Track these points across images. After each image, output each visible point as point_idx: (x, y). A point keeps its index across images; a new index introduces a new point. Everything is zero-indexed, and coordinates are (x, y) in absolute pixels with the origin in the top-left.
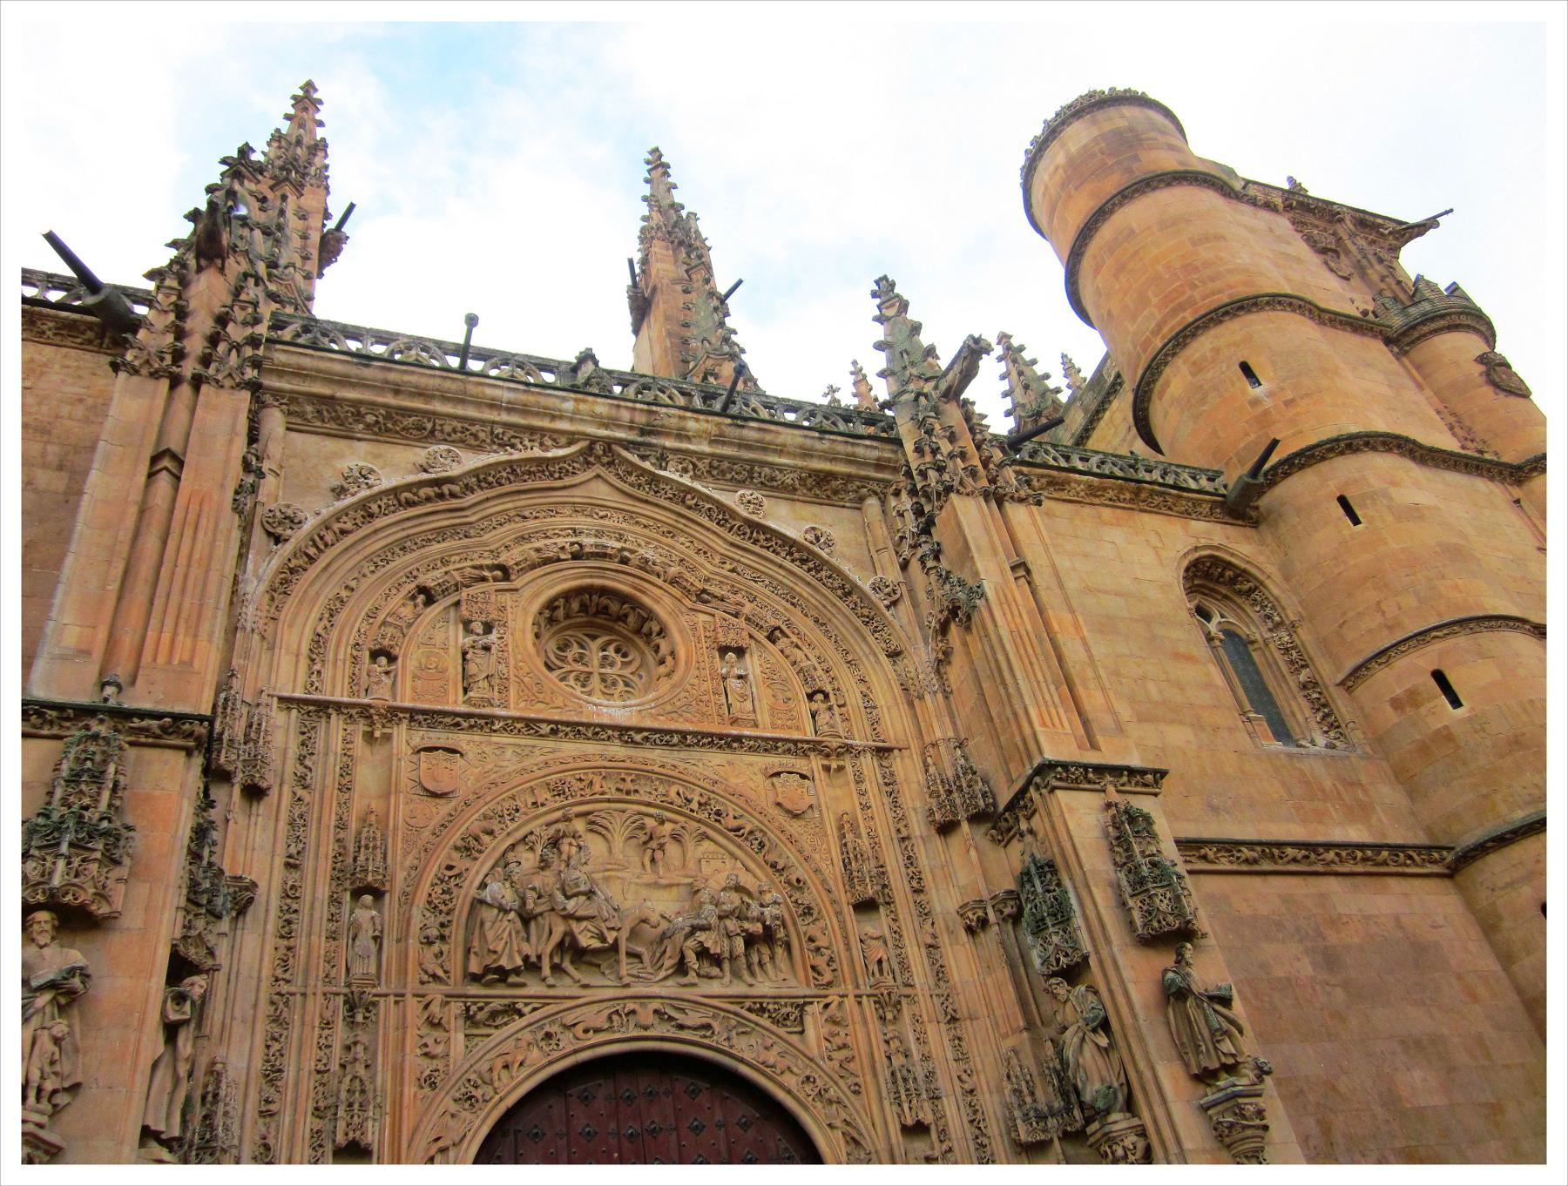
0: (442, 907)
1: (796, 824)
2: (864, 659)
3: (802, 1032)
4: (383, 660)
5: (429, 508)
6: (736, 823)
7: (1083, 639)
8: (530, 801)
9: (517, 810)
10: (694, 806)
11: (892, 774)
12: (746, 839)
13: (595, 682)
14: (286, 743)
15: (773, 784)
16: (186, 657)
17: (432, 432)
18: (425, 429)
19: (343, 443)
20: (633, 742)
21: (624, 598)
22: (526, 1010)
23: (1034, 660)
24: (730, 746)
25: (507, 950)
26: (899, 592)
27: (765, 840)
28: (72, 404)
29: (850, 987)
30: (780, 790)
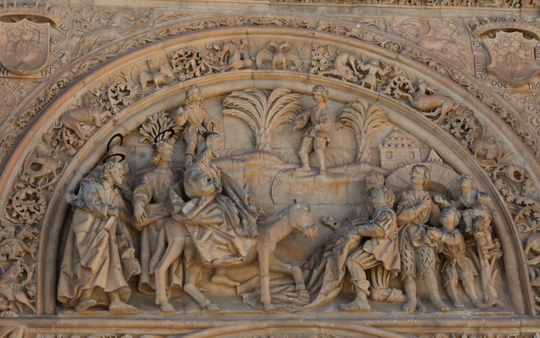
0: (25, 215)
8: (145, 78)
9: (127, 92)
10: (371, 80)
12: (445, 122)
15: (484, 46)
27: (471, 123)
30: (493, 54)
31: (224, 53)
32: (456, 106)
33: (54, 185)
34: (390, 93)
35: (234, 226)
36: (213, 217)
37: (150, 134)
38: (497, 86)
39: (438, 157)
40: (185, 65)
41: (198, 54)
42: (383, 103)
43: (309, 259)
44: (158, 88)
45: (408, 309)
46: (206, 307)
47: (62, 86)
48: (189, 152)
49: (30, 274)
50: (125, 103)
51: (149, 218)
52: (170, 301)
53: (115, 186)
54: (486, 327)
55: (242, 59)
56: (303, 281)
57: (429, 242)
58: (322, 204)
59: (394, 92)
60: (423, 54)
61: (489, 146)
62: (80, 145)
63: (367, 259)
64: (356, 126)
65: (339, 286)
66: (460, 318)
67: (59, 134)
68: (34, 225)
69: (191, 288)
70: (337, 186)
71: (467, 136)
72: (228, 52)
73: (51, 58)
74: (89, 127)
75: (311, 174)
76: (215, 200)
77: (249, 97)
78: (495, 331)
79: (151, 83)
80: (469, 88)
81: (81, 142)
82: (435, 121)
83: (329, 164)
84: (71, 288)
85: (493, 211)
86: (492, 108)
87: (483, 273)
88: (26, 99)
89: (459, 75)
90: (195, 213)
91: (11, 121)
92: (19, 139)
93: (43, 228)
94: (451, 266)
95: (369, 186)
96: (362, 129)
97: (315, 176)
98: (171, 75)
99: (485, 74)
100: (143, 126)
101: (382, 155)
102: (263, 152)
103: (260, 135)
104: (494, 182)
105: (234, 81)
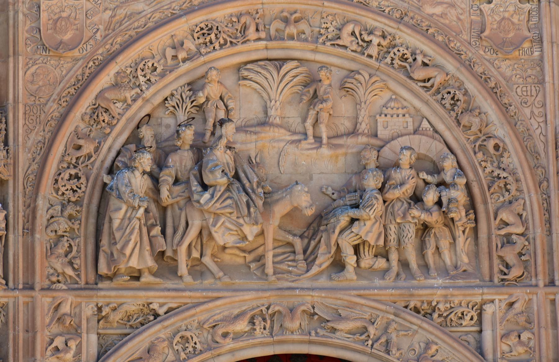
0: (69, 194)
1: (506, 67)
3: (481, 331)
8: (170, 53)
10: (373, 50)
22: (161, 311)
27: (459, 95)
29: (541, 284)
30: (489, 20)
31: (241, 25)
32: (449, 76)
33: (93, 164)
34: (389, 62)
35: (243, 216)
36: (226, 207)
37: (174, 107)
38: (489, 53)
39: (429, 126)
40: (205, 39)
41: (217, 27)
42: (383, 73)
43: (309, 226)
44: (181, 64)
45: (388, 278)
46: (220, 278)
47: (97, 64)
48: (208, 128)
49: (75, 249)
50: (153, 80)
51: (173, 198)
52: (190, 273)
53: (144, 173)
54: (453, 295)
55: (257, 30)
56: (302, 252)
57: (410, 219)
58: (323, 173)
59: (394, 62)
60: (424, 20)
61: (474, 119)
62: (113, 124)
63: (355, 238)
64: (357, 96)
65: (332, 257)
66: (432, 287)
67: (96, 114)
68: (76, 203)
69: (207, 260)
70: (337, 157)
71: (456, 108)
72: (245, 23)
73: (87, 34)
74: (121, 104)
75: (314, 146)
76: (228, 189)
77: (262, 71)
78: (461, 298)
79: (175, 57)
80: (462, 57)
81: (115, 122)
82: (428, 93)
83: (332, 134)
84: (109, 267)
85: (472, 181)
86: (481, 77)
87: (457, 242)
88: (66, 78)
89: (455, 43)
90: (210, 204)
91: (54, 100)
93: (85, 205)
94: (430, 235)
95: (364, 162)
96: (363, 100)
97: (317, 148)
98: (193, 48)
99: (480, 41)
100: (168, 99)
101: (379, 124)
102: (272, 125)
103: (271, 108)
104: (475, 153)
105: (249, 51)
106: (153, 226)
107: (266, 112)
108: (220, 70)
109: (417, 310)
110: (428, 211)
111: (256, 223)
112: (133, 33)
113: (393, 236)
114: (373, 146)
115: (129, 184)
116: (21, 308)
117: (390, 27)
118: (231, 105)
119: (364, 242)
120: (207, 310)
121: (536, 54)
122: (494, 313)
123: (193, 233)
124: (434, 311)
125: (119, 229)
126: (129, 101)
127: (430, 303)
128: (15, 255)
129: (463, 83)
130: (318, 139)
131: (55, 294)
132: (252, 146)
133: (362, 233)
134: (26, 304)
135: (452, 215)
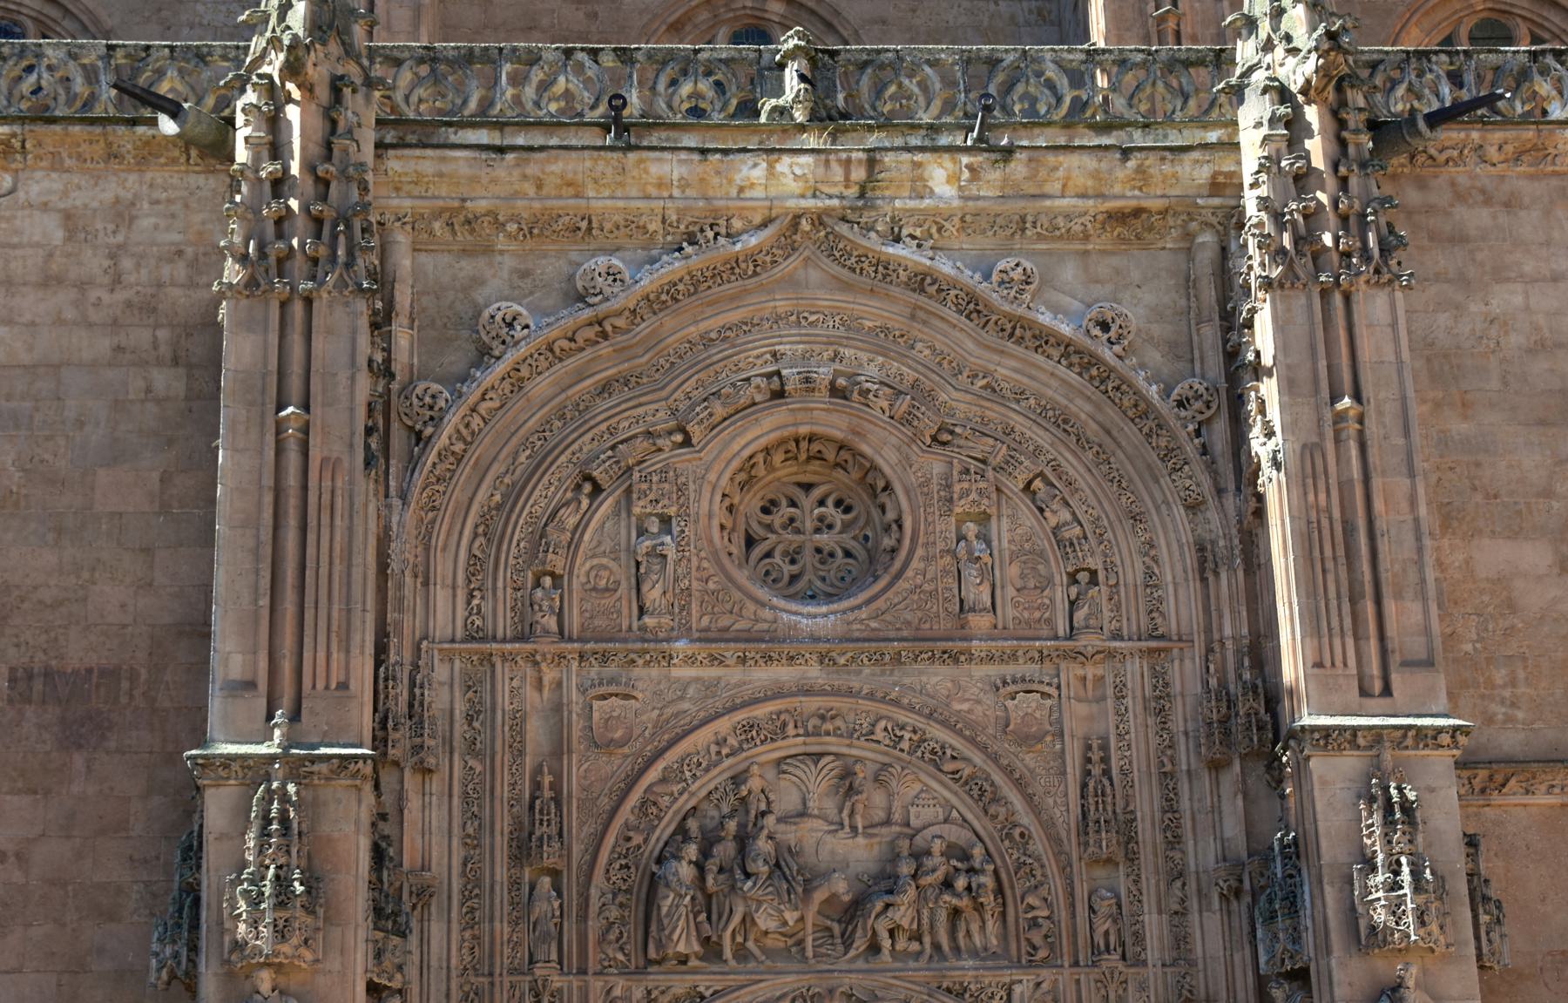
1: (1029, 759)
2: (1153, 511)
4: (547, 581)
5: (589, 353)
6: (949, 767)
7: (1416, 520)
8: (714, 748)
10: (905, 745)
11: (1166, 685)
13: (808, 558)
14: (452, 702)
16: (342, 679)
17: (590, 229)
18: (579, 229)
19: (481, 262)
20: (835, 664)
21: (842, 447)
22: (707, 994)
23: (1330, 565)
24: (956, 661)
25: (684, 935)
26: (1214, 406)
27: (986, 786)
28: (171, 261)
29: (1066, 964)
30: (1013, 715)
33: (642, 854)
43: (846, 911)
49: (625, 935)
52: (734, 957)
53: (690, 862)
54: (983, 976)
55: (796, 727)
66: (963, 969)
69: (750, 944)
70: (872, 845)
73: (637, 732)
76: (769, 877)
79: (719, 753)
83: (867, 823)
92: (614, 811)
97: (853, 837)
98: (736, 744)
102: (810, 816)
106: (700, 912)
107: (804, 804)
108: (761, 765)
109: (949, 990)
110: (959, 896)
111: (797, 909)
112: (679, 730)
113: (925, 921)
114: (906, 835)
115: (676, 873)
116: (575, 992)
117: (920, 722)
118: (772, 797)
119: (899, 926)
120: (752, 992)
121: (1058, 747)
122: (1022, 993)
123: (737, 919)
124: (965, 991)
125: (667, 915)
126: (676, 795)
127: (961, 984)
128: (570, 942)
129: (989, 775)
130: (854, 828)
131: (607, 978)
132: (791, 836)
133: (897, 918)
134: (580, 988)
135: (982, 900)
